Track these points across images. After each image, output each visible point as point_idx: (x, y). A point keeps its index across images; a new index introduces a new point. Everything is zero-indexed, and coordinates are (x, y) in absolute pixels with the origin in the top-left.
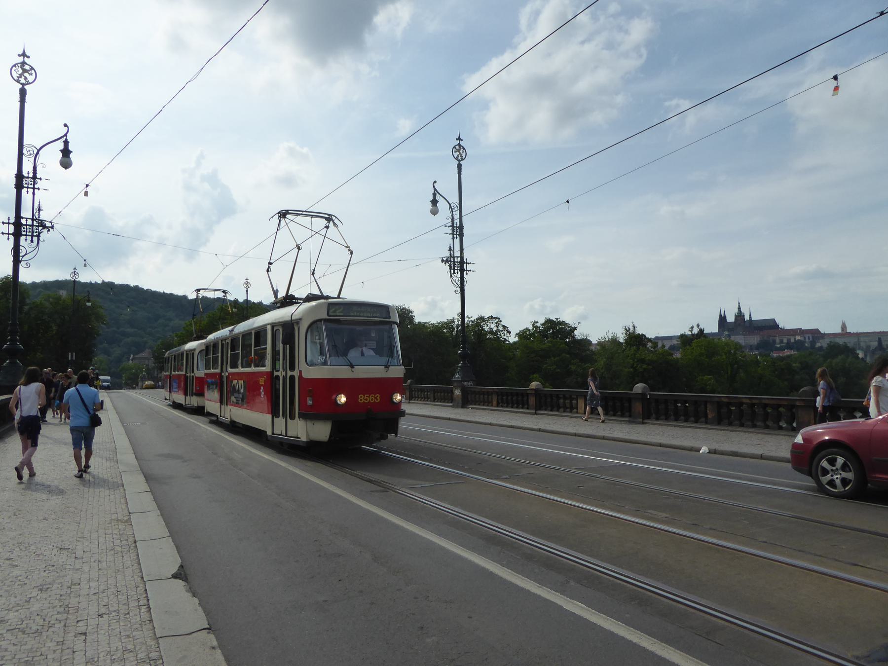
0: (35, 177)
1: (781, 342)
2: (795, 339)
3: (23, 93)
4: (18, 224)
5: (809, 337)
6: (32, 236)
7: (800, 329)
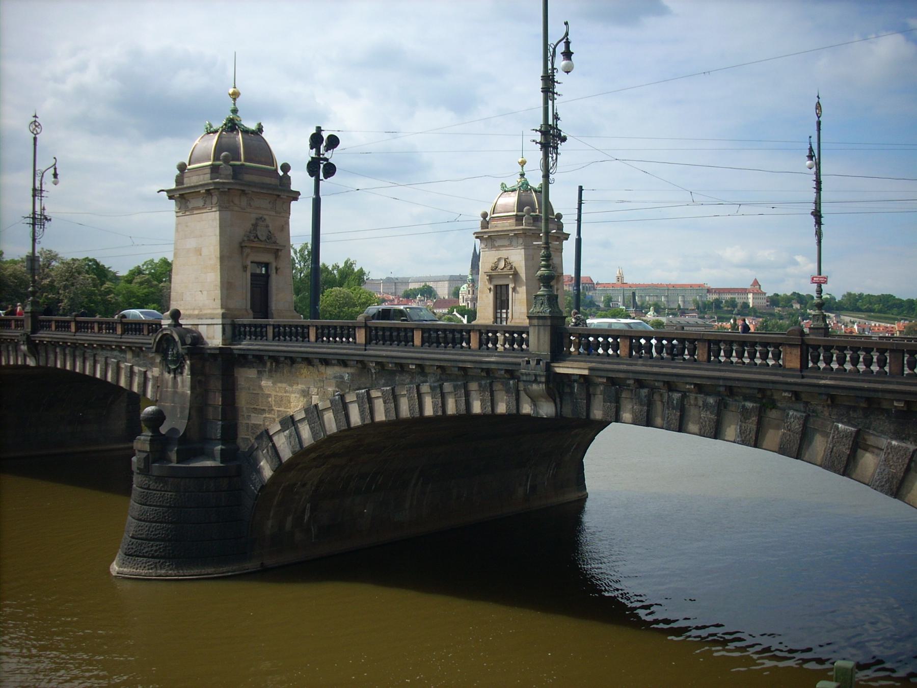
0: (41, 190)
3: (35, 139)
4: (34, 218)
6: (41, 225)
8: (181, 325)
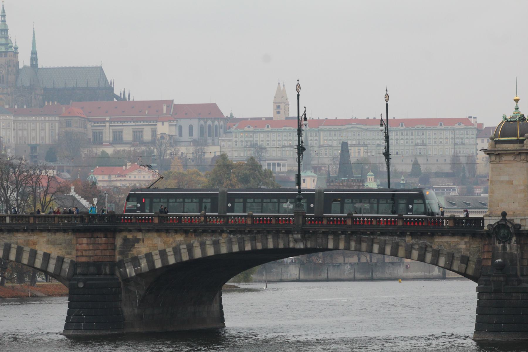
1: (118, 139)
2: (154, 132)
3: (298, 95)
4: (298, 149)
5: (191, 128)
7: (169, 103)
8: (507, 219)
